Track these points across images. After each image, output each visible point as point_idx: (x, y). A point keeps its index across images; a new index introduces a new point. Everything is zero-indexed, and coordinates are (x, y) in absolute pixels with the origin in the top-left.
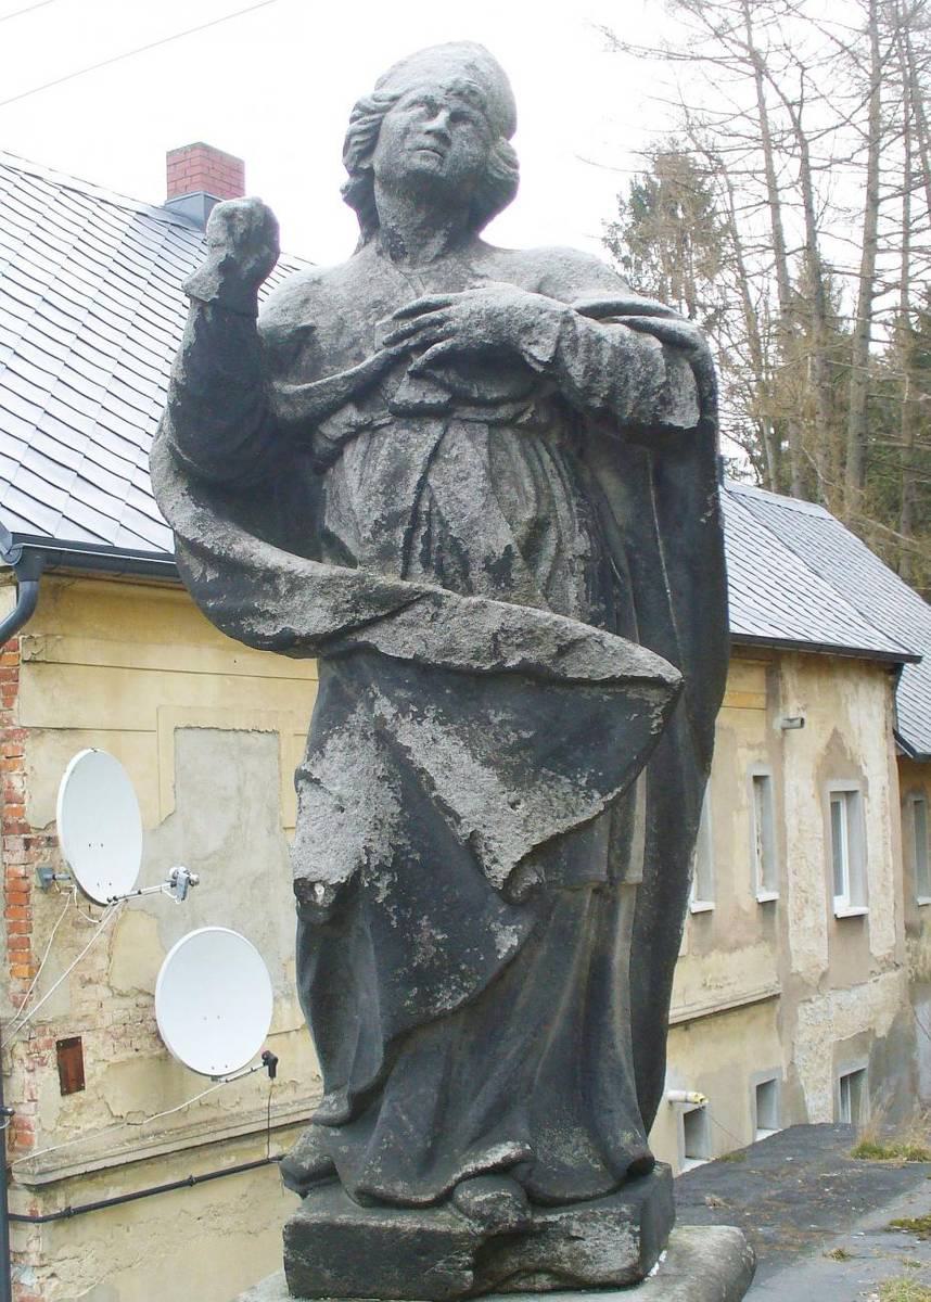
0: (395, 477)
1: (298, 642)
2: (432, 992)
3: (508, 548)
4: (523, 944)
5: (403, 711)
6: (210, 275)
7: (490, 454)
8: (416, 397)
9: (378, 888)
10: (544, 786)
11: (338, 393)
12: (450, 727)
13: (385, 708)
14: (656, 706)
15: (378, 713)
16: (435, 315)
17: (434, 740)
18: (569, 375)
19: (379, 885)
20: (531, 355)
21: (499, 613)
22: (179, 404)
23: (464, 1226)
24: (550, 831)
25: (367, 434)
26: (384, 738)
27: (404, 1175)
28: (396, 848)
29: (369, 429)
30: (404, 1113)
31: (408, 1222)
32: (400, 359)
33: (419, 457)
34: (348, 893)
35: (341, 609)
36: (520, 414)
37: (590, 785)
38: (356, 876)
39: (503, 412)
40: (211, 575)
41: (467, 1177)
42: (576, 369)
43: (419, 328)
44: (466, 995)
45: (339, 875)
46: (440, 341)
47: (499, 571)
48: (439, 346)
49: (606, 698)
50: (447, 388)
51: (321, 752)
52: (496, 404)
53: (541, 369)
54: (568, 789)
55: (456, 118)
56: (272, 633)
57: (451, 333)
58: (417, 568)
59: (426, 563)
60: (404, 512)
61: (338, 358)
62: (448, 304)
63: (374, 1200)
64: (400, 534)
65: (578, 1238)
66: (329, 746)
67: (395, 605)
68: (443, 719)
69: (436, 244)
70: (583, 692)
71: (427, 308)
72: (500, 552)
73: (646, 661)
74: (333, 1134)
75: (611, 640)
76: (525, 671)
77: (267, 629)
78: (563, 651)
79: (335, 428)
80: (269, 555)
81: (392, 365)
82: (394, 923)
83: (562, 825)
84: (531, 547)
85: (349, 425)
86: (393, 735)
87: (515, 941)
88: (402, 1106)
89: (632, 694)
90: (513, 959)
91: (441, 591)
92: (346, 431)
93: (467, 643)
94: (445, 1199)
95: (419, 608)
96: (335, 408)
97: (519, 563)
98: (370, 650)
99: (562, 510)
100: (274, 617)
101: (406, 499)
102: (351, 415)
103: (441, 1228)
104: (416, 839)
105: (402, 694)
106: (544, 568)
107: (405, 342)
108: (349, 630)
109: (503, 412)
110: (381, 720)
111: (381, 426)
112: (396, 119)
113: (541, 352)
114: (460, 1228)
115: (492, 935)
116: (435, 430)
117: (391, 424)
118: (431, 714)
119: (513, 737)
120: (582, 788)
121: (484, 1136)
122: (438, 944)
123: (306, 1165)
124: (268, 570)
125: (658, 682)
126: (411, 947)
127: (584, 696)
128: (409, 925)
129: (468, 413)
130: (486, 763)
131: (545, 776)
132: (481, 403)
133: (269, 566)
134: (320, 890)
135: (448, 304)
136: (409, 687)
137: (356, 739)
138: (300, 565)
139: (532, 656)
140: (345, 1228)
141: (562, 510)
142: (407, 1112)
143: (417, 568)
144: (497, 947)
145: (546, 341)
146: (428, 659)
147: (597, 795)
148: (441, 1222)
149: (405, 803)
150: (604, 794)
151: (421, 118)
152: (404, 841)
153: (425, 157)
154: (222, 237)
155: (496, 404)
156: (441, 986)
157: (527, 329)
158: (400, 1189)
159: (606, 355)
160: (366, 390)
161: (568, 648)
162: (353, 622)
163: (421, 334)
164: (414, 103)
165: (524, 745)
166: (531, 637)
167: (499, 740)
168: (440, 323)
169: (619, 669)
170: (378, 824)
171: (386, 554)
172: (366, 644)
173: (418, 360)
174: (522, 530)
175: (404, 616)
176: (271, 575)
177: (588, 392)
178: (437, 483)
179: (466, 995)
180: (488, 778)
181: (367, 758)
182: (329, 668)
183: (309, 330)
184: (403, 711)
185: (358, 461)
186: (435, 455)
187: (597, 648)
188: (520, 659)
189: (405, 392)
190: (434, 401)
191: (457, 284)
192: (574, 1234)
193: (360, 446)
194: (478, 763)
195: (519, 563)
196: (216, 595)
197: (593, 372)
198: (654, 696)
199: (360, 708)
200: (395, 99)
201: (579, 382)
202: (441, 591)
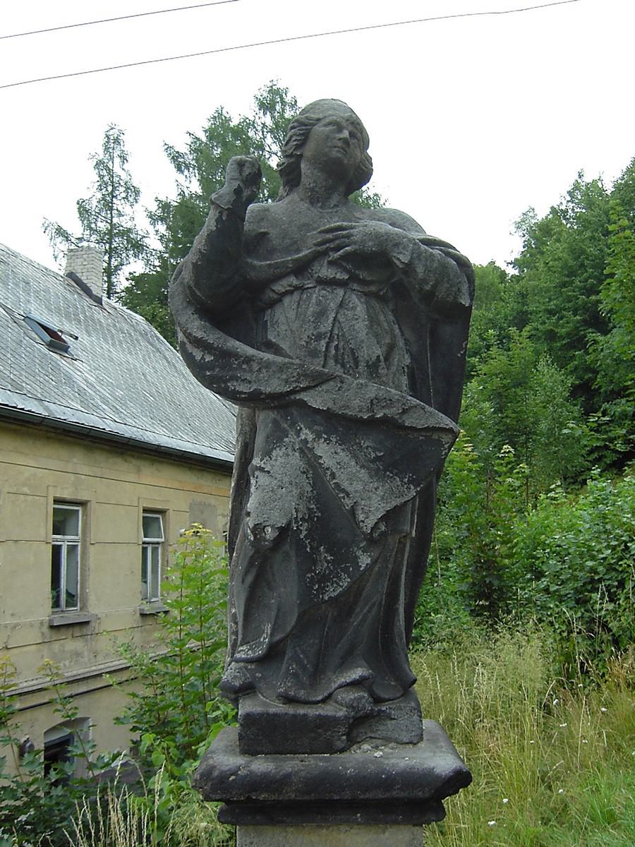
1: (262, 397)
2: (324, 587)
3: (378, 357)
4: (374, 562)
5: (319, 436)
6: (228, 194)
8: (332, 274)
9: (301, 530)
10: (388, 481)
11: (287, 268)
12: (343, 447)
13: (307, 434)
14: (446, 444)
15: (303, 438)
16: (344, 232)
17: (335, 453)
18: (416, 271)
19: (302, 528)
20: (398, 259)
22: (199, 263)
23: (342, 713)
24: (394, 504)
25: (300, 291)
26: (305, 450)
27: (302, 686)
28: (309, 509)
30: (302, 653)
35: (289, 380)
36: (381, 290)
37: (409, 482)
38: (289, 524)
39: (373, 288)
40: (209, 358)
41: (341, 687)
42: (420, 270)
43: (337, 238)
44: (341, 589)
45: (282, 522)
46: (348, 246)
47: (373, 368)
49: (421, 438)
50: (348, 272)
51: (270, 457)
53: (401, 266)
54: (399, 483)
56: (248, 391)
57: (355, 243)
58: (331, 362)
59: (336, 361)
60: (326, 333)
62: (352, 228)
63: (288, 700)
64: (323, 343)
65: (394, 719)
66: (274, 453)
67: (319, 380)
68: (342, 442)
69: (335, 199)
70: (409, 434)
72: (374, 359)
74: (249, 667)
76: (385, 420)
77: (244, 388)
78: (404, 411)
79: (279, 287)
81: (317, 256)
82: (308, 549)
83: (399, 501)
85: (290, 286)
86: (311, 450)
87: (369, 561)
88: (300, 650)
92: (288, 288)
93: (356, 402)
95: (331, 383)
97: (382, 364)
98: (303, 404)
100: (250, 382)
102: (293, 280)
103: (330, 713)
104: (319, 506)
107: (328, 245)
108: (294, 392)
109: (373, 288)
110: (305, 441)
111: (308, 288)
112: (319, 129)
114: (341, 714)
115: (357, 557)
116: (340, 292)
117: (315, 287)
118: (334, 440)
119: (373, 455)
120: (406, 484)
121: (344, 664)
122: (328, 562)
123: (237, 684)
124: (247, 357)
126: (315, 562)
127: (410, 436)
128: (315, 550)
129: (355, 286)
130: (363, 467)
131: (389, 476)
132: (363, 282)
133: (248, 354)
135: (352, 228)
136: (321, 425)
137: (290, 450)
139: (390, 412)
140: (275, 715)
142: (303, 652)
143: (331, 362)
144: (360, 564)
145: (406, 253)
146: (334, 411)
147: (412, 487)
148: (328, 710)
149: (314, 486)
150: (416, 487)
152: (313, 506)
153: (338, 151)
154: (236, 175)
156: (329, 584)
157: (397, 245)
158: (302, 694)
160: (301, 268)
162: (296, 387)
163: (337, 242)
164: (329, 124)
165: (377, 459)
166: (390, 402)
167: (367, 456)
168: (348, 236)
170: (301, 496)
172: (301, 400)
174: (384, 349)
176: (248, 360)
177: (424, 281)
178: (344, 320)
179: (341, 589)
181: (296, 459)
182: (271, 413)
183: (265, 234)
184: (319, 436)
185: (295, 305)
186: (341, 305)
187: (422, 411)
188: (382, 414)
189: (326, 272)
190: (341, 278)
192: (393, 717)
193: (296, 296)
194: (358, 466)
195: (382, 364)
196: (212, 369)
197: (428, 270)
199: (292, 433)
200: (319, 120)
201: (421, 275)
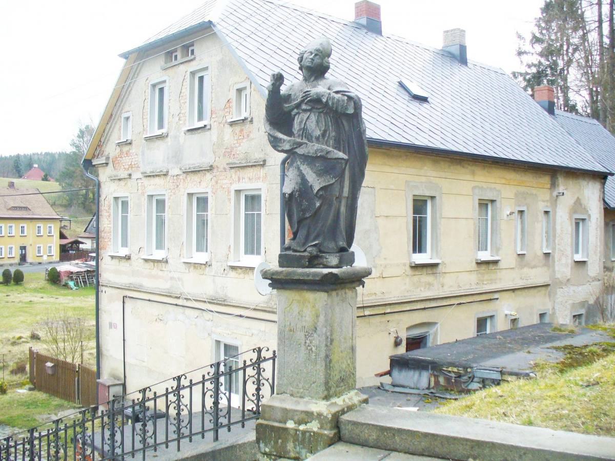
0: (301, 122)
5: (301, 163)
7: (318, 118)
16: (309, 93)
21: (317, 146)
24: (324, 185)
29: (298, 113)
31: (298, 254)
32: (304, 100)
33: (305, 119)
34: (291, 195)
37: (332, 178)
38: (292, 193)
39: (321, 110)
41: (309, 246)
42: (330, 103)
43: (306, 95)
47: (317, 139)
48: (309, 99)
52: (319, 109)
55: (316, 55)
57: (311, 96)
58: (304, 138)
59: (305, 137)
61: (294, 100)
62: (310, 91)
64: (301, 132)
67: (300, 145)
68: (308, 165)
69: (313, 79)
71: (307, 91)
72: (318, 135)
73: (341, 155)
75: (335, 151)
76: (321, 157)
77: (280, 149)
79: (293, 113)
80: (280, 136)
81: (302, 102)
83: (327, 184)
84: (324, 135)
89: (340, 161)
90: (320, 207)
91: (307, 142)
93: (311, 151)
94: (305, 251)
95: (304, 145)
96: (293, 109)
97: (321, 137)
98: (296, 153)
99: (330, 128)
101: (303, 126)
102: (295, 111)
105: (302, 160)
106: (326, 139)
108: (292, 149)
109: (321, 110)
112: (305, 56)
113: (324, 100)
116: (309, 113)
121: (314, 240)
125: (343, 159)
126: (302, 205)
130: (314, 173)
132: (317, 109)
134: (287, 195)
138: (285, 137)
141: (330, 128)
143: (304, 138)
149: (302, 180)
151: (309, 55)
155: (319, 109)
157: (323, 96)
158: (298, 249)
159: (335, 100)
160: (298, 106)
161: (328, 152)
164: (309, 52)
166: (322, 150)
168: (310, 94)
169: (336, 156)
170: (297, 183)
171: (299, 136)
173: (306, 101)
174: (322, 132)
175: (302, 147)
176: (281, 139)
180: (314, 175)
181: (296, 172)
191: (315, 87)
195: (321, 137)
197: (333, 104)
198: (343, 161)
199: (295, 163)
200: (306, 51)
202: (307, 142)
